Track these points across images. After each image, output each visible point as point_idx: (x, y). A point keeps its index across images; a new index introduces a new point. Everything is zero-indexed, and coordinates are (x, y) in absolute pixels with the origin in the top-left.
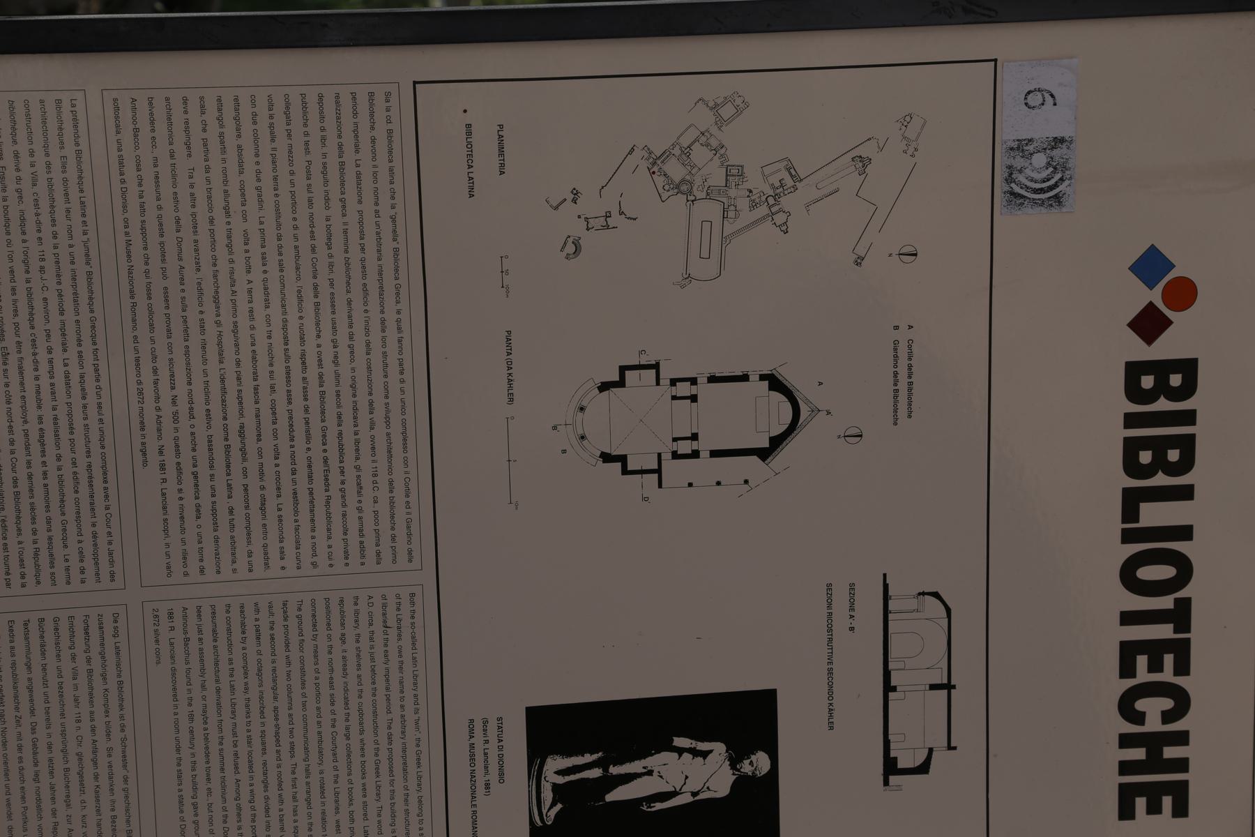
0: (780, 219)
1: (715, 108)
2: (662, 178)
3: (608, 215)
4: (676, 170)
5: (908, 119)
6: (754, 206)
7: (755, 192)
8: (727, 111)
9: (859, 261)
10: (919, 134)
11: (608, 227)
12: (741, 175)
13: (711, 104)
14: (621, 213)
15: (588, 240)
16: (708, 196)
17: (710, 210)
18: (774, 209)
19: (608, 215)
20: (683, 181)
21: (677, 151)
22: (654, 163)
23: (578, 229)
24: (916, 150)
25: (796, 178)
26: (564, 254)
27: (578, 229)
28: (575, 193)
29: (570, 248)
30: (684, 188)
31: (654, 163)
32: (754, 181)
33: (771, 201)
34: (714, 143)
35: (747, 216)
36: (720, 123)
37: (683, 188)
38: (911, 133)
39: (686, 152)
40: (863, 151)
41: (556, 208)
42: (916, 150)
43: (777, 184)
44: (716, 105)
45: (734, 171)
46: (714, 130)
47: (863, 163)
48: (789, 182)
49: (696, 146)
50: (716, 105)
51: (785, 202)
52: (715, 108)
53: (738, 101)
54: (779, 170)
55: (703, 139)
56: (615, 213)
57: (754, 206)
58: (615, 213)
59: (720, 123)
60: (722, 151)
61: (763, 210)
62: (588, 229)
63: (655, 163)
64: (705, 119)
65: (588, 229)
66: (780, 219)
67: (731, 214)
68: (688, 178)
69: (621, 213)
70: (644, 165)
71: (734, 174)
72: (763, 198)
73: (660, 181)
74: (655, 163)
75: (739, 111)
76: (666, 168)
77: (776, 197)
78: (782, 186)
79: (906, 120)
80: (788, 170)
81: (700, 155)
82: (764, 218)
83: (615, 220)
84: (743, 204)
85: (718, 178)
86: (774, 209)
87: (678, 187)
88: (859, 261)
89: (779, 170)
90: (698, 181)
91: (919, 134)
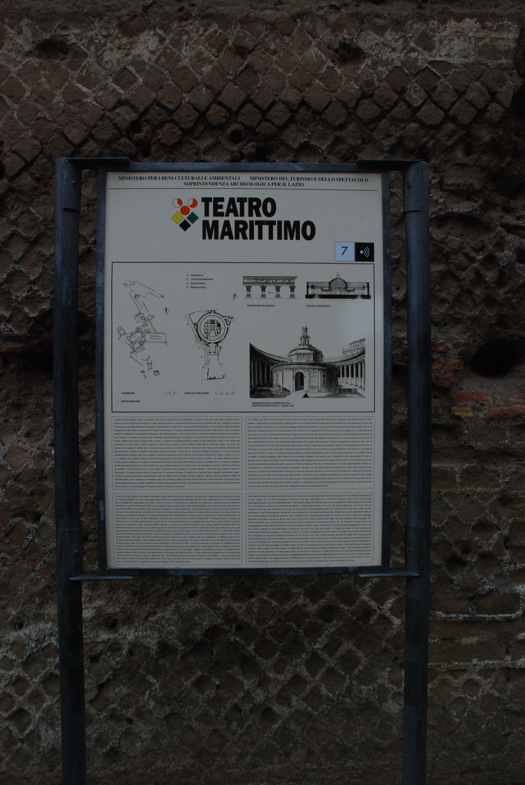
0: (150, 318)
3: (148, 363)
4: (137, 345)
6: (147, 325)
8: (122, 332)
9: (162, 296)
12: (138, 328)
16: (144, 337)
17: (147, 337)
19: (148, 363)
23: (151, 371)
25: (140, 314)
27: (151, 371)
28: (142, 372)
29: (157, 373)
32: (140, 325)
35: (149, 327)
36: (125, 334)
37: (142, 343)
38: (128, 283)
40: (133, 295)
47: (136, 296)
48: (141, 315)
51: (146, 316)
57: (147, 325)
59: (125, 334)
61: (148, 322)
63: (134, 351)
64: (124, 338)
66: (150, 318)
70: (135, 354)
71: (138, 330)
73: (139, 349)
74: (134, 351)
75: (122, 329)
79: (126, 285)
81: (133, 339)
83: (149, 361)
84: (146, 328)
85: (139, 334)
88: (162, 296)
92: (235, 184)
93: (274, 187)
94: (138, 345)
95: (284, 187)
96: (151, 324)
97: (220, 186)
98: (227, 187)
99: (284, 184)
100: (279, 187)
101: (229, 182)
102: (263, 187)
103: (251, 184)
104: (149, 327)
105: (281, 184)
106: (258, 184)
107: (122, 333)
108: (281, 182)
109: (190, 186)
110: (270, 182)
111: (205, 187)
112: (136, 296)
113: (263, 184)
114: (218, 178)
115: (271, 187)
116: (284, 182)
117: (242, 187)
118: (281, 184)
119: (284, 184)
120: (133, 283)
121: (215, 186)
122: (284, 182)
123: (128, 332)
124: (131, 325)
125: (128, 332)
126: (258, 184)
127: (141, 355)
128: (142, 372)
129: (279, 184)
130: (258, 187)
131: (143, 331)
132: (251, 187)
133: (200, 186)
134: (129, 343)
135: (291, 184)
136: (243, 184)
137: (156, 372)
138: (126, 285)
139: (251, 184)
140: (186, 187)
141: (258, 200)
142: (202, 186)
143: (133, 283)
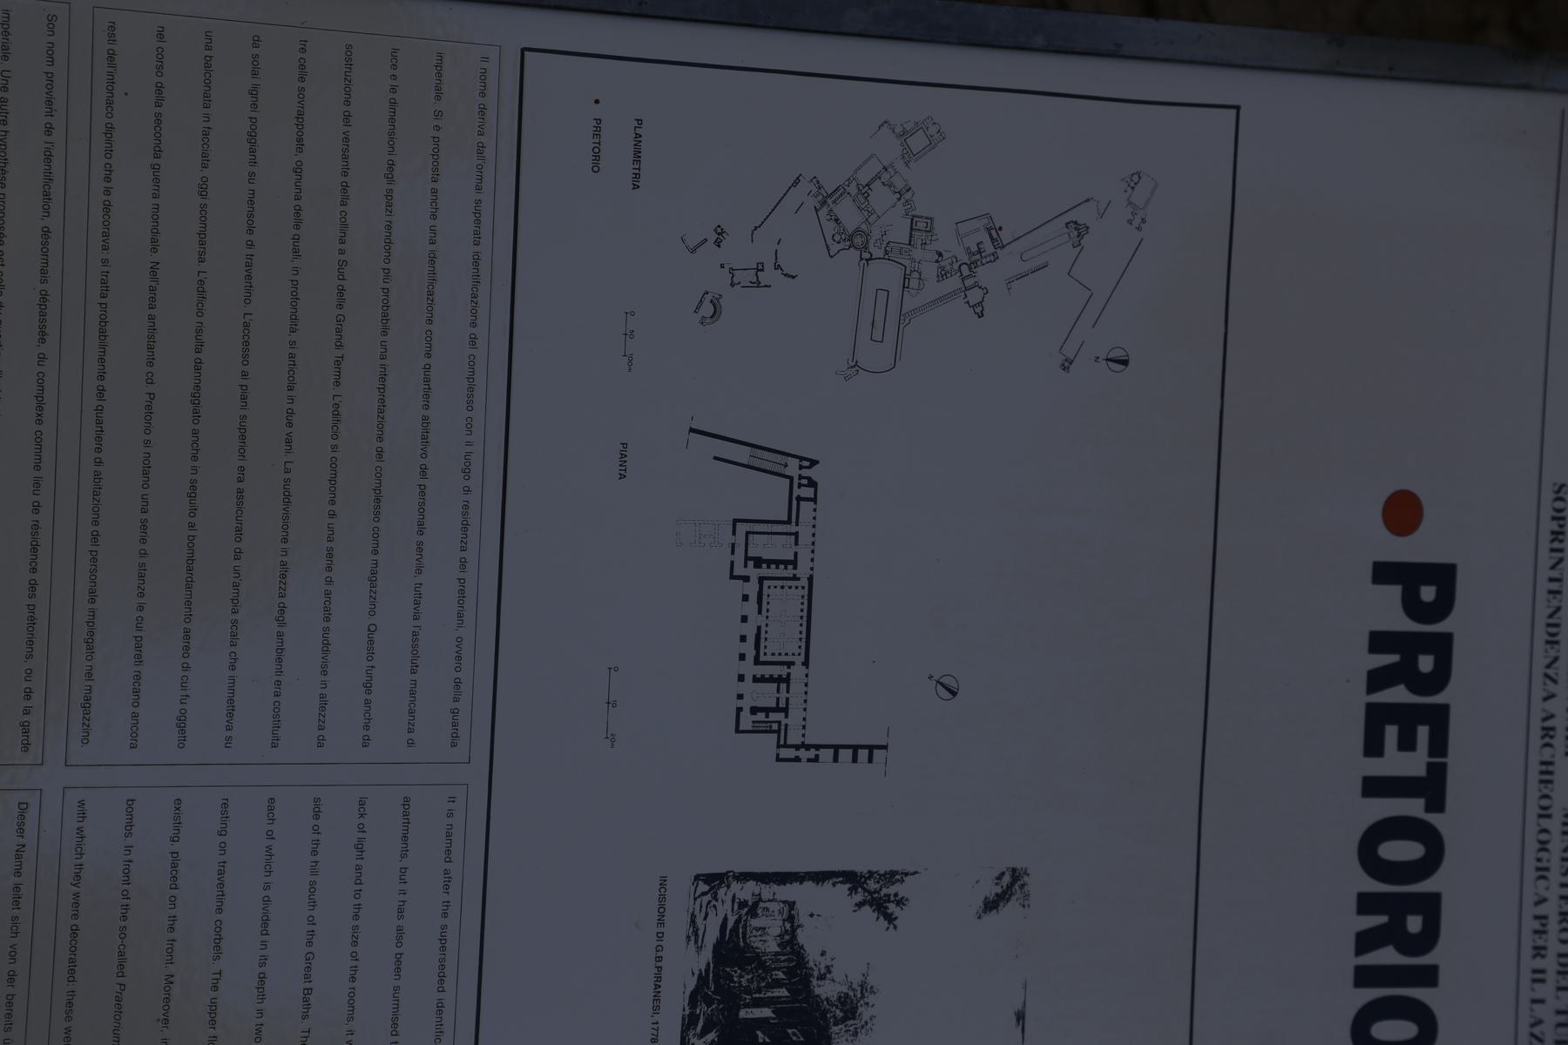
1: (904, 135)
2: (833, 224)
3: (760, 268)
4: (850, 215)
5: (1136, 178)
6: (943, 275)
7: (946, 255)
8: (917, 142)
9: (1066, 365)
10: (1148, 201)
11: (758, 284)
12: (930, 231)
13: (899, 130)
14: (777, 267)
16: (887, 255)
17: (886, 275)
18: (969, 282)
19: (760, 268)
20: (858, 230)
21: (853, 189)
22: (824, 203)
24: (1143, 221)
26: (699, 316)
28: (720, 232)
29: (707, 309)
30: (858, 240)
31: (824, 203)
33: (965, 270)
34: (899, 185)
36: (908, 156)
37: (856, 240)
39: (865, 190)
40: (1077, 216)
41: (693, 251)
42: (1143, 221)
43: (974, 249)
44: (904, 132)
45: (921, 225)
46: (900, 165)
47: (1080, 230)
48: (989, 247)
49: (877, 185)
50: (904, 132)
51: (985, 274)
52: (904, 135)
53: (933, 130)
54: (978, 230)
55: (885, 177)
56: (769, 267)
57: (943, 275)
58: (769, 267)
59: (908, 156)
60: (908, 196)
61: (954, 283)
62: (732, 285)
63: (826, 199)
65: (732, 285)
67: (914, 283)
68: (864, 227)
69: (777, 267)
70: (811, 203)
71: (921, 227)
72: (956, 266)
73: (830, 228)
74: (826, 199)
76: (838, 210)
77: (972, 265)
78: (979, 252)
80: (989, 230)
81: (881, 197)
82: (954, 293)
84: (930, 270)
85: (900, 233)
86: (969, 282)
87: (851, 238)
88: (1066, 365)
89: (978, 230)
90: (876, 234)
91: (1148, 201)
92: (1548, 732)
93: (1530, 925)
95: (1526, 976)
96: (951, 295)
97: (1540, 661)
98: (1538, 693)
99: (1538, 976)
100: (1527, 951)
102: (1531, 874)
103: (1545, 813)
105: (1539, 963)
106: (1543, 846)
109: (1547, 512)
111: (1544, 586)
112: (1080, 230)
113: (1542, 872)
115: (1530, 910)
116: (1551, 976)
117: (1535, 768)
118: (1539, 963)
119: (1538, 976)
121: (1541, 635)
122: (1551, 976)
126: (1543, 846)
128: (720, 232)
129: (1539, 951)
130: (1532, 846)
131: (917, 253)
132: (1533, 810)
133: (1546, 560)
134: (864, 178)
135: (1539, 1010)
137: (715, 304)
139: (1545, 813)
140: (1548, 495)
142: (1545, 573)
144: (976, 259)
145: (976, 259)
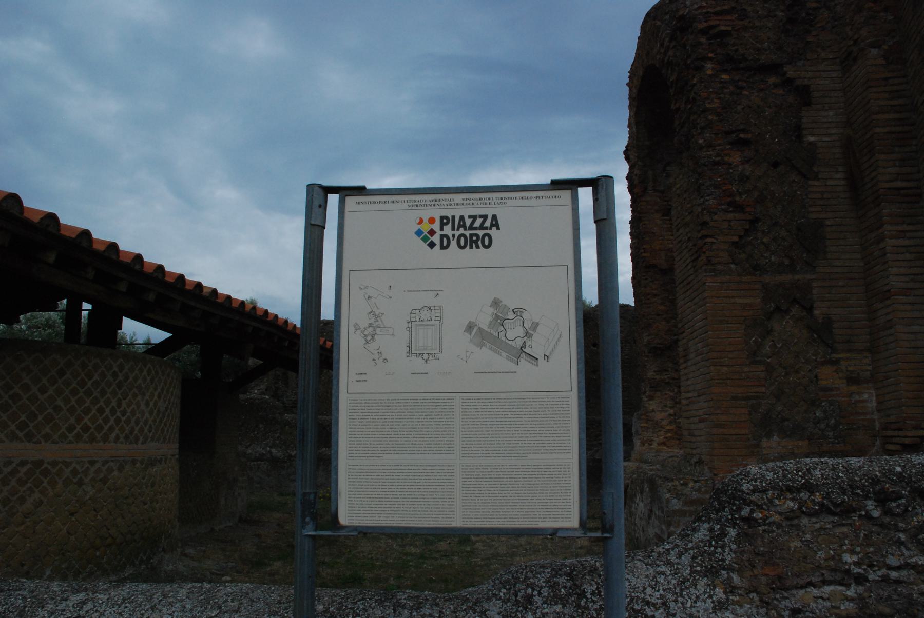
4: (369, 338)
15: (384, 357)
17: (378, 330)
32: (372, 321)
39: (365, 336)
47: (369, 297)
64: (359, 332)
71: (370, 325)
74: (367, 342)
79: (361, 289)
81: (366, 333)
94: (369, 339)
99: (490, 203)
101: (445, 203)
104: (380, 322)
107: (357, 327)
108: (488, 201)
110: (479, 202)
112: (369, 297)
114: (436, 200)
119: (490, 203)
120: (367, 287)
123: (362, 327)
124: (364, 321)
125: (362, 327)
127: (373, 346)
136: (456, 204)
138: (361, 289)
141: (447, 218)
143: (367, 287)
144: (375, 315)
145: (375, 315)
